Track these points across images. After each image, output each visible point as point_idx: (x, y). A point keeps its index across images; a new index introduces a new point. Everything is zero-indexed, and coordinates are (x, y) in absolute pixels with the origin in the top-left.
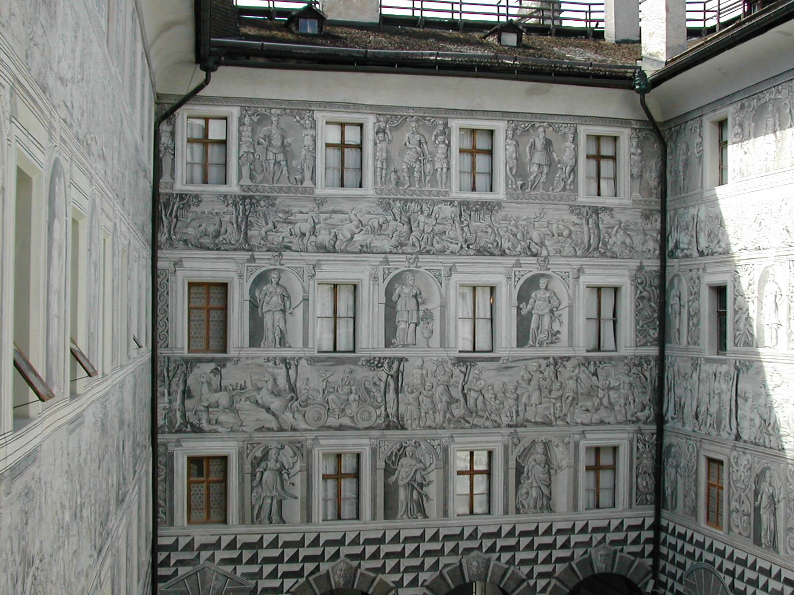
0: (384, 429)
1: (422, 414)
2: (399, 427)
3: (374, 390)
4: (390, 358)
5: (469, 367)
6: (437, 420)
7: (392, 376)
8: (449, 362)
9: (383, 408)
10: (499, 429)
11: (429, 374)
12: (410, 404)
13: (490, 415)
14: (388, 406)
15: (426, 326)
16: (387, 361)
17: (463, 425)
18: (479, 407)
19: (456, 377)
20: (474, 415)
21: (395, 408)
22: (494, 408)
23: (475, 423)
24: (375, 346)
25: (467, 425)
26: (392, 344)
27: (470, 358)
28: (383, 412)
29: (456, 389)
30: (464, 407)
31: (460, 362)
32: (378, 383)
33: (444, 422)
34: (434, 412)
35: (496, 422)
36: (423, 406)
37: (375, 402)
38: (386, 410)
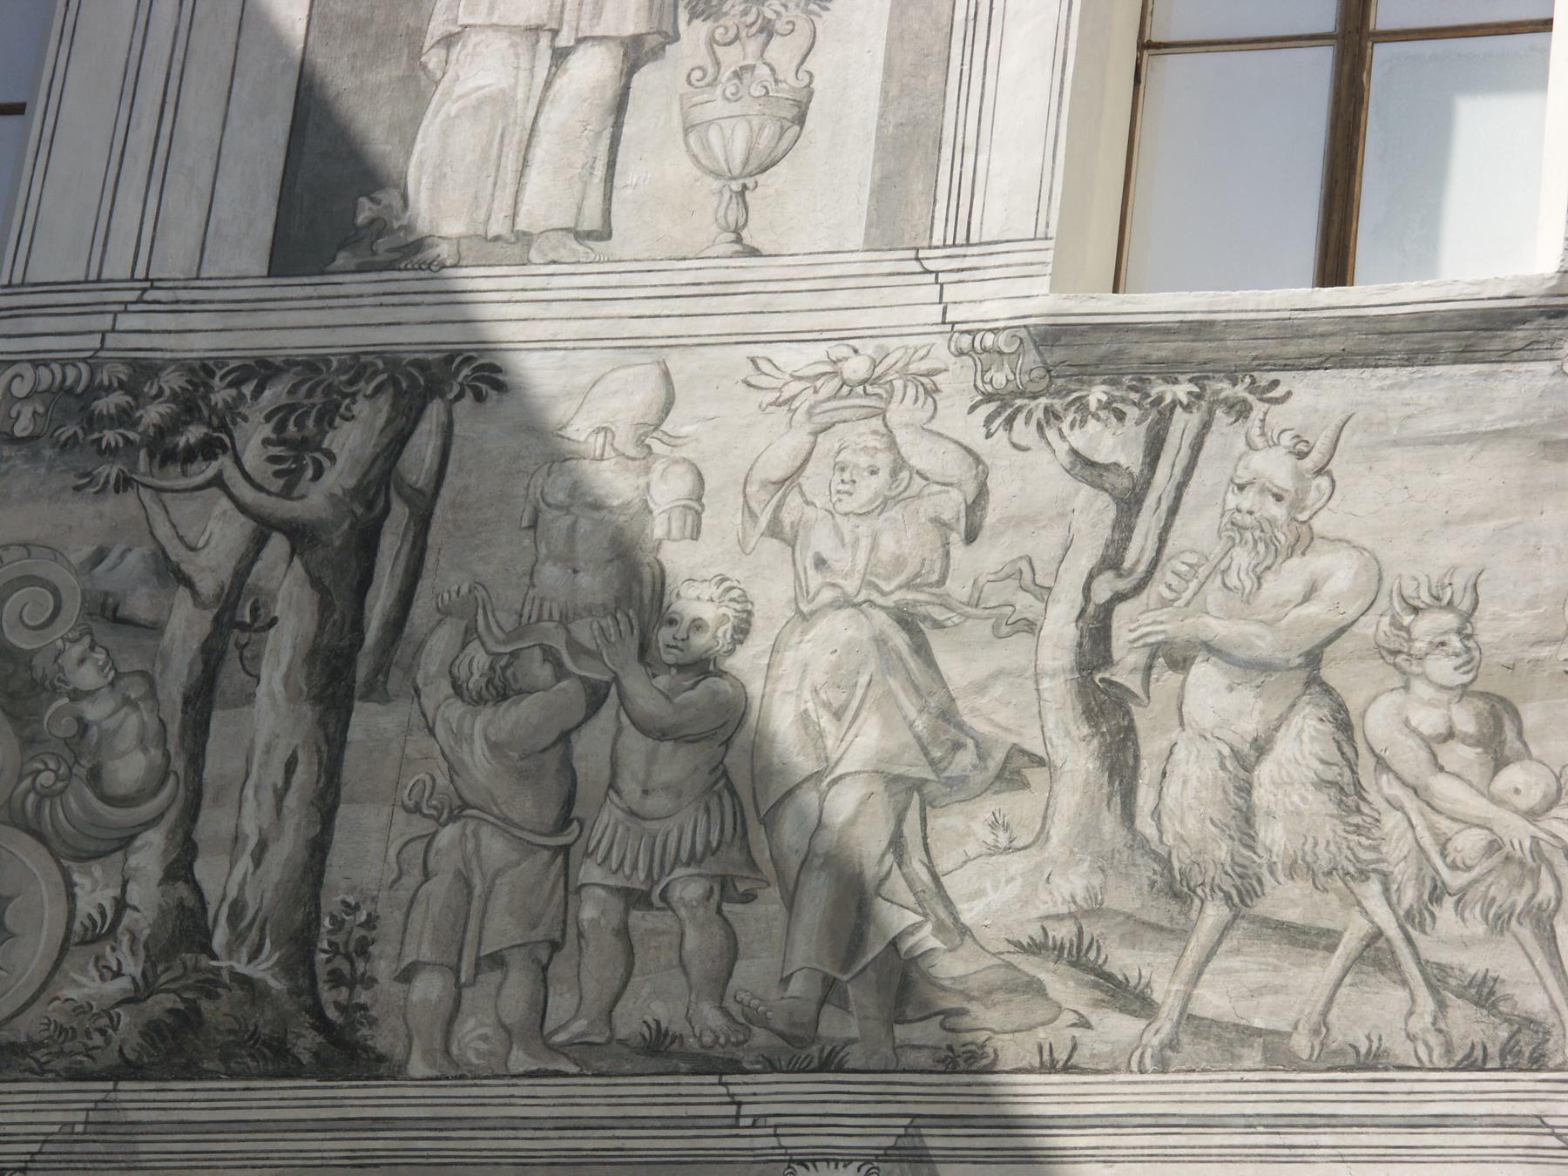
0: (127, 1070)
1: (588, 913)
2: (306, 1042)
3: (87, 677)
4: (311, 366)
5: (1183, 425)
6: (751, 975)
7: (300, 536)
8: (957, 381)
9: (149, 855)
10: (1525, 1080)
11: (723, 515)
12: (458, 809)
13: (1413, 920)
14: (213, 823)
15: (731, 57)
16: (274, 394)
17: (1059, 1036)
18: (1274, 836)
19: (1016, 522)
20: (1214, 913)
21: (286, 849)
22: (1468, 843)
23: (1212, 1000)
24: (174, 259)
25: (1117, 1027)
26: (352, 237)
27: (1199, 329)
28: (146, 895)
29: (1015, 652)
30: (1087, 834)
31: (1084, 373)
32: (140, 605)
33: (830, 992)
34: (726, 889)
35: (1484, 993)
36: (607, 820)
37: (79, 799)
38: (180, 867)
